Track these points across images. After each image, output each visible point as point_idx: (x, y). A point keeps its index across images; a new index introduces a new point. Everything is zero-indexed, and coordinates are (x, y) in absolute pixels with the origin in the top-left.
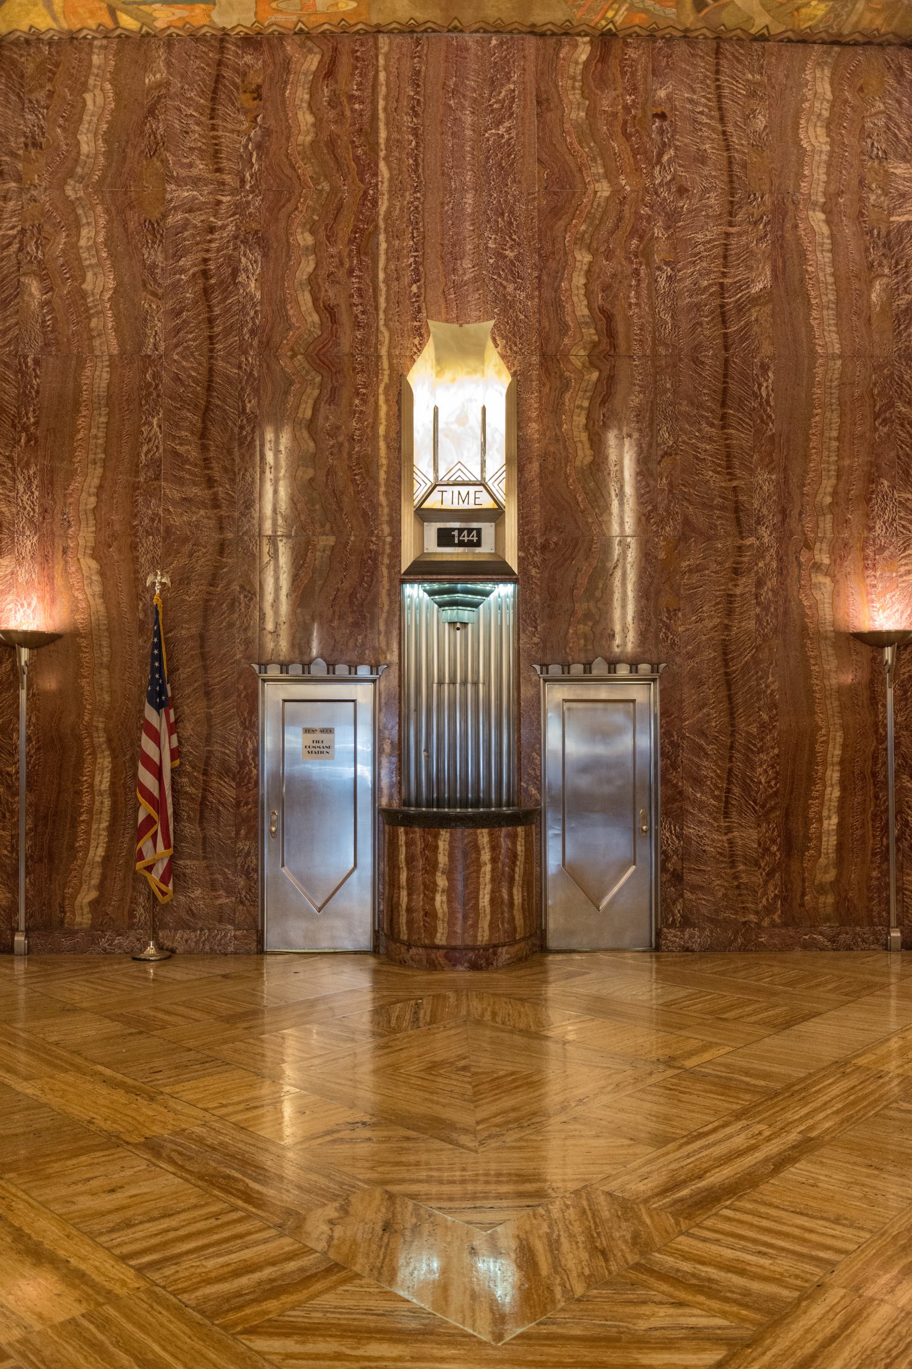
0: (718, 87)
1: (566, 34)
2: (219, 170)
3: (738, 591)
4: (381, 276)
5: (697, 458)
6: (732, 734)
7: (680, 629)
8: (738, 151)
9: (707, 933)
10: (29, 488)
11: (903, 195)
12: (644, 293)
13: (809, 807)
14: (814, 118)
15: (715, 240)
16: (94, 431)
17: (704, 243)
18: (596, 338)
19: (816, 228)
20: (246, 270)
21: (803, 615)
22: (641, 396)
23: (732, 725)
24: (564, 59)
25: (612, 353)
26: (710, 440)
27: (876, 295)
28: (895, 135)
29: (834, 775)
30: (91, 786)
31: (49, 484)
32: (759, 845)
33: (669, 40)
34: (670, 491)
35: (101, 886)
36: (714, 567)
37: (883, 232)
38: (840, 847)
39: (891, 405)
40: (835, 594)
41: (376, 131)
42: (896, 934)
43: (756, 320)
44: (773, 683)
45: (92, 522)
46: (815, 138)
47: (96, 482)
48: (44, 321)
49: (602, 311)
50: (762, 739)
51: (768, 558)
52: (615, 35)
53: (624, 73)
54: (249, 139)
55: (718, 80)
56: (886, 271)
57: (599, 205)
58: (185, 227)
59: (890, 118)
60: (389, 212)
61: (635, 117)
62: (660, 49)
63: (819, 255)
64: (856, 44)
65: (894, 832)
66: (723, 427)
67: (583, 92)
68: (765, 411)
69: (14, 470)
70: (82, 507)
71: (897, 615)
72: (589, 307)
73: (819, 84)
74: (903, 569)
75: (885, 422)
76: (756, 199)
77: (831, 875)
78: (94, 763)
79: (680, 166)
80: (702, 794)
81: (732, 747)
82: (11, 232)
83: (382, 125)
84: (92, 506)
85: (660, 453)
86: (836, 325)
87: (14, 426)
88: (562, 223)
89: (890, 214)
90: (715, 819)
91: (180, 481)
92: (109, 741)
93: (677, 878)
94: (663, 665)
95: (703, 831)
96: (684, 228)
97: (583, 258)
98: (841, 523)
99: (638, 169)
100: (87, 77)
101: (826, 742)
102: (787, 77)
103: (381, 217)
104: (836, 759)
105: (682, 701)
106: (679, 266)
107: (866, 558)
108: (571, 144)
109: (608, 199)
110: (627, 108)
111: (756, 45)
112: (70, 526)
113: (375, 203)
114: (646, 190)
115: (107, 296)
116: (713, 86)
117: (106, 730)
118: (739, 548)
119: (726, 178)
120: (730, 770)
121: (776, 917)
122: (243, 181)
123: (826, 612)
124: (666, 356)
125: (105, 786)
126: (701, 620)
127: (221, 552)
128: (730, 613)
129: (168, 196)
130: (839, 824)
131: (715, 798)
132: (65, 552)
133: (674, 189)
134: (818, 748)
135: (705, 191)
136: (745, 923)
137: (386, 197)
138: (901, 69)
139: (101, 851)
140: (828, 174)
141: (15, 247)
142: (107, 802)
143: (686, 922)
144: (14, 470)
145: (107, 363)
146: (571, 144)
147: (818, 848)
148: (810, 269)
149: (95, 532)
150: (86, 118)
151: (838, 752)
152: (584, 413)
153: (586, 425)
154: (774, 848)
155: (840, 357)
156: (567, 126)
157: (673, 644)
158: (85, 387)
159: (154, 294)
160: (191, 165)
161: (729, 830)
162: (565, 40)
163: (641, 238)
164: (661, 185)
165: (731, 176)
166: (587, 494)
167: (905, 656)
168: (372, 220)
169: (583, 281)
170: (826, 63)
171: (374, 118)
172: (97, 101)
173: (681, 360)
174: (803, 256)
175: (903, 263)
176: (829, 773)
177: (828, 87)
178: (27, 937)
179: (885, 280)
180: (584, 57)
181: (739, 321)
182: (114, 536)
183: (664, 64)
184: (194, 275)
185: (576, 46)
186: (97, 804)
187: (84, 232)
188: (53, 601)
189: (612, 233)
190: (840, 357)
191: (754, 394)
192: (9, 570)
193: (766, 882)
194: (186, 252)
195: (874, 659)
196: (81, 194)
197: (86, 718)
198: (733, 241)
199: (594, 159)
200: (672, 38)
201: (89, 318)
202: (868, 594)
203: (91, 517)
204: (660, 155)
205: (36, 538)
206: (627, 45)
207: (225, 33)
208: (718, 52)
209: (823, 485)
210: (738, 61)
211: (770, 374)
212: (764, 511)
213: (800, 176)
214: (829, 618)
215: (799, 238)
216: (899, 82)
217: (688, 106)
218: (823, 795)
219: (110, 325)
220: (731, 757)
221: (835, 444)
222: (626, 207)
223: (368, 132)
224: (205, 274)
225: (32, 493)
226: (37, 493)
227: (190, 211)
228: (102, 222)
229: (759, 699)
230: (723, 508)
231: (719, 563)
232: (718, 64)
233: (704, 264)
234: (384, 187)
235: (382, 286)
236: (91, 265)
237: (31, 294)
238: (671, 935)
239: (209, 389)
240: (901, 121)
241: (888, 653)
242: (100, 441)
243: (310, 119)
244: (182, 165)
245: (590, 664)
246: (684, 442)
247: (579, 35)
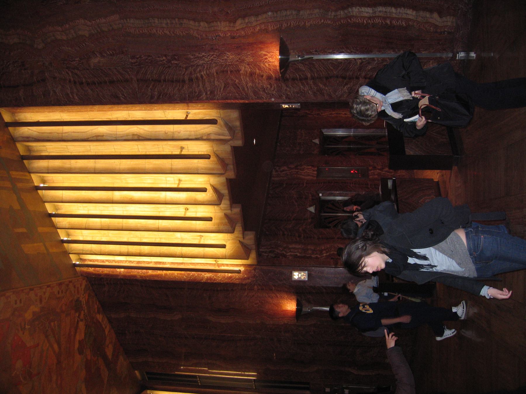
10: (201, 58)
16: (164, 25)
30: (370, 18)
35: (431, 11)
45: (215, 24)
47: (191, 22)
69: (192, 66)
78: (356, 17)
82: (70, 74)
84: (206, 25)
87: (169, 67)
92: (343, 8)
112: (219, 36)
117: (336, 11)
125: (370, 10)
132: (233, 38)
139: (410, 12)
141: (76, 71)
142: (380, 9)
144: (192, 66)
145: (125, 20)
149: (220, 22)
158: (141, 31)
186: (381, 14)
187: (59, 37)
188: (262, 43)
192: (247, 66)
197: (329, 22)
203: (212, 24)
219: (104, 20)
225: (203, 56)
226: (203, 54)
237: (99, 62)
242: (169, 22)
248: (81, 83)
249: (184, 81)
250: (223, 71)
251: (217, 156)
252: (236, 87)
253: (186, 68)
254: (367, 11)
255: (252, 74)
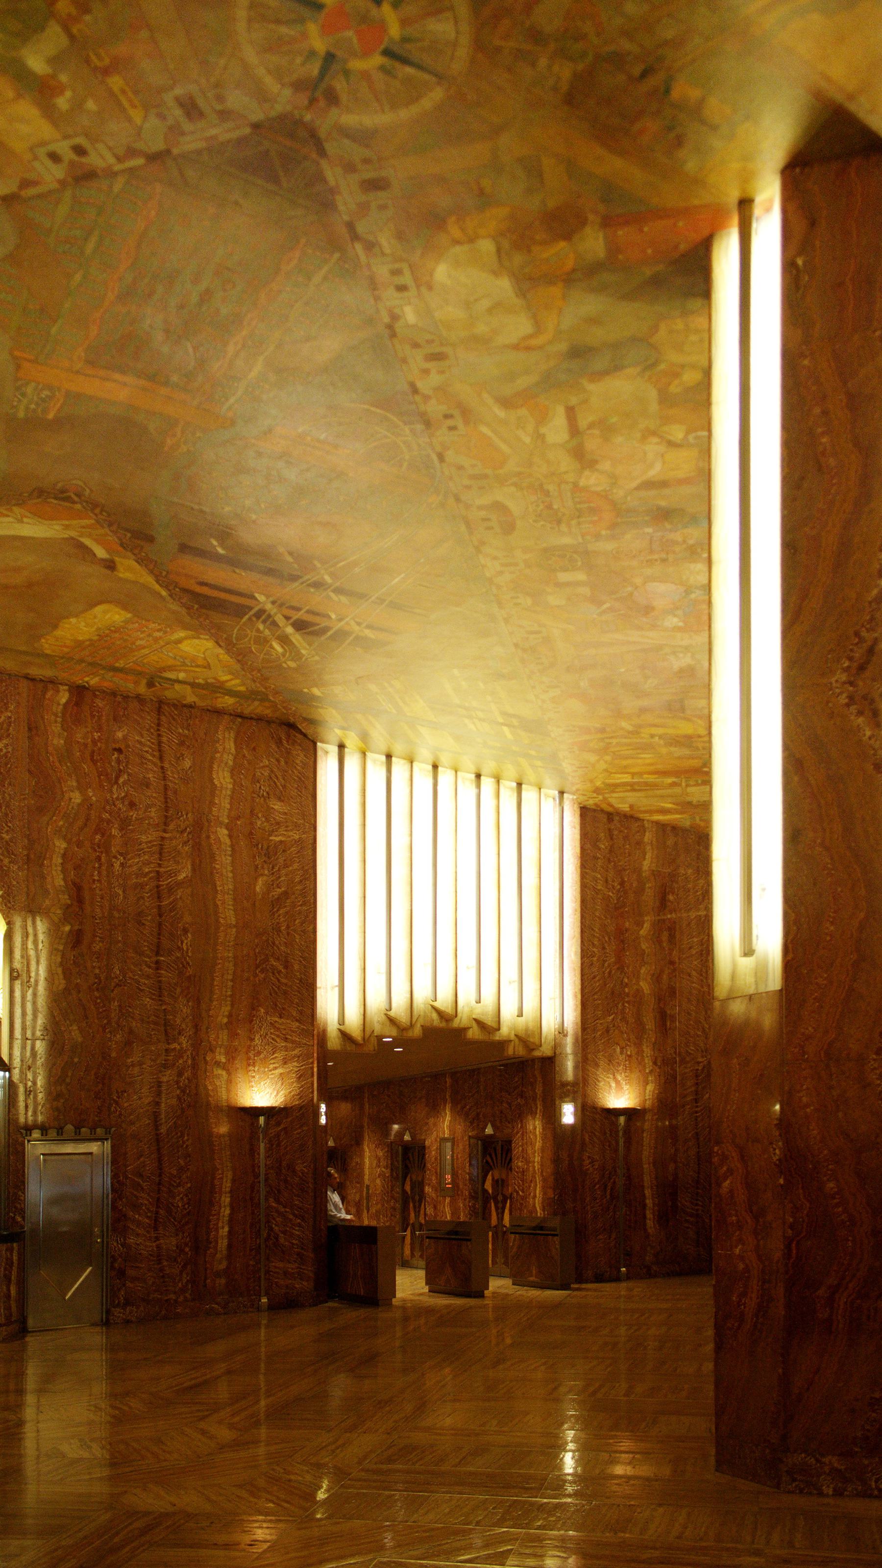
0: (159, 735)
1: (52, 682)
3: (165, 1079)
5: (138, 988)
6: (160, 1175)
7: (126, 1105)
8: (171, 781)
9: (142, 1308)
11: (278, 823)
12: (104, 873)
13: (210, 1221)
14: (223, 765)
15: (154, 841)
17: (146, 843)
18: (69, 902)
19: (222, 839)
21: (208, 1095)
22: (101, 944)
23: (161, 1169)
24: (49, 699)
25: (80, 913)
26: (148, 977)
27: (259, 887)
28: (275, 783)
29: (226, 1200)
32: (177, 1247)
33: (126, 698)
34: (120, 1011)
36: (149, 1063)
37: (265, 846)
38: (230, 1246)
39: (266, 960)
40: (229, 1081)
42: (264, 1300)
43: (181, 898)
44: (188, 1140)
46: (223, 778)
49: (74, 884)
50: (180, 1178)
51: (185, 1057)
52: (87, 689)
53: (93, 716)
55: (158, 730)
56: (266, 872)
57: (73, 808)
59: (272, 771)
61: (100, 749)
62: (119, 703)
63: (224, 858)
64: (251, 718)
65: (265, 1234)
66: (157, 969)
67: (62, 725)
68: (185, 959)
71: (268, 1096)
72: (64, 879)
73: (227, 744)
74: (271, 1066)
75: (262, 971)
76: (182, 816)
77: (223, 1265)
79: (131, 787)
80: (139, 1215)
81: (159, 1184)
85: (113, 984)
86: (233, 905)
88: (45, 819)
89: (270, 835)
90: (148, 1232)
93: (122, 1273)
94: (113, 1129)
95: (140, 1241)
96: (133, 831)
97: (61, 845)
98: (233, 1035)
99: (101, 786)
101: (222, 1178)
102: (205, 734)
104: (228, 1190)
105: (126, 1154)
106: (129, 857)
107: (249, 1058)
108: (53, 762)
109: (79, 805)
110: (94, 742)
111: (185, 710)
114: (107, 801)
116: (155, 733)
118: (166, 1050)
119: (163, 799)
120: (158, 1199)
121: (187, 1295)
123: (224, 1095)
124: (119, 918)
126: (140, 1098)
128: (159, 1094)
130: (230, 1232)
131: (148, 1217)
133: (126, 803)
134: (216, 1182)
135: (148, 806)
136: (167, 1300)
138: (280, 739)
140: (231, 804)
143: (127, 1303)
146: (53, 762)
147: (216, 1248)
148: (217, 866)
151: (229, 1185)
152: (60, 953)
153: (61, 963)
154: (187, 1249)
155: (235, 926)
156: (50, 749)
157: (121, 1114)
161: (157, 1239)
162: (50, 686)
163: (103, 835)
164: (117, 799)
165: (166, 798)
166: (60, 1010)
167: (272, 1122)
169: (60, 861)
170: (232, 728)
173: (129, 921)
174: (212, 857)
175: (276, 868)
176: (223, 1199)
177: (232, 745)
179: (265, 878)
180: (64, 701)
181: (169, 897)
183: (121, 713)
185: (58, 691)
189: (81, 829)
190: (235, 926)
191: (179, 948)
193: (181, 1273)
195: (252, 1124)
198: (167, 842)
199: (70, 775)
200: (128, 697)
202: (250, 1082)
204: (117, 778)
206: (95, 696)
208: (159, 711)
209: (223, 1010)
210: (174, 719)
211: (189, 935)
212: (184, 1026)
213: (212, 803)
214: (224, 1097)
215: (210, 845)
216: (278, 747)
217: (138, 746)
218: (219, 1214)
220: (159, 1190)
221: (230, 984)
222: (92, 812)
229: (178, 1151)
230: (155, 1023)
231: (153, 1060)
232: (159, 719)
233: (146, 857)
238: (117, 1312)
240: (279, 774)
241: (262, 1120)
245: (62, 1128)
246: (130, 978)
247: (61, 684)
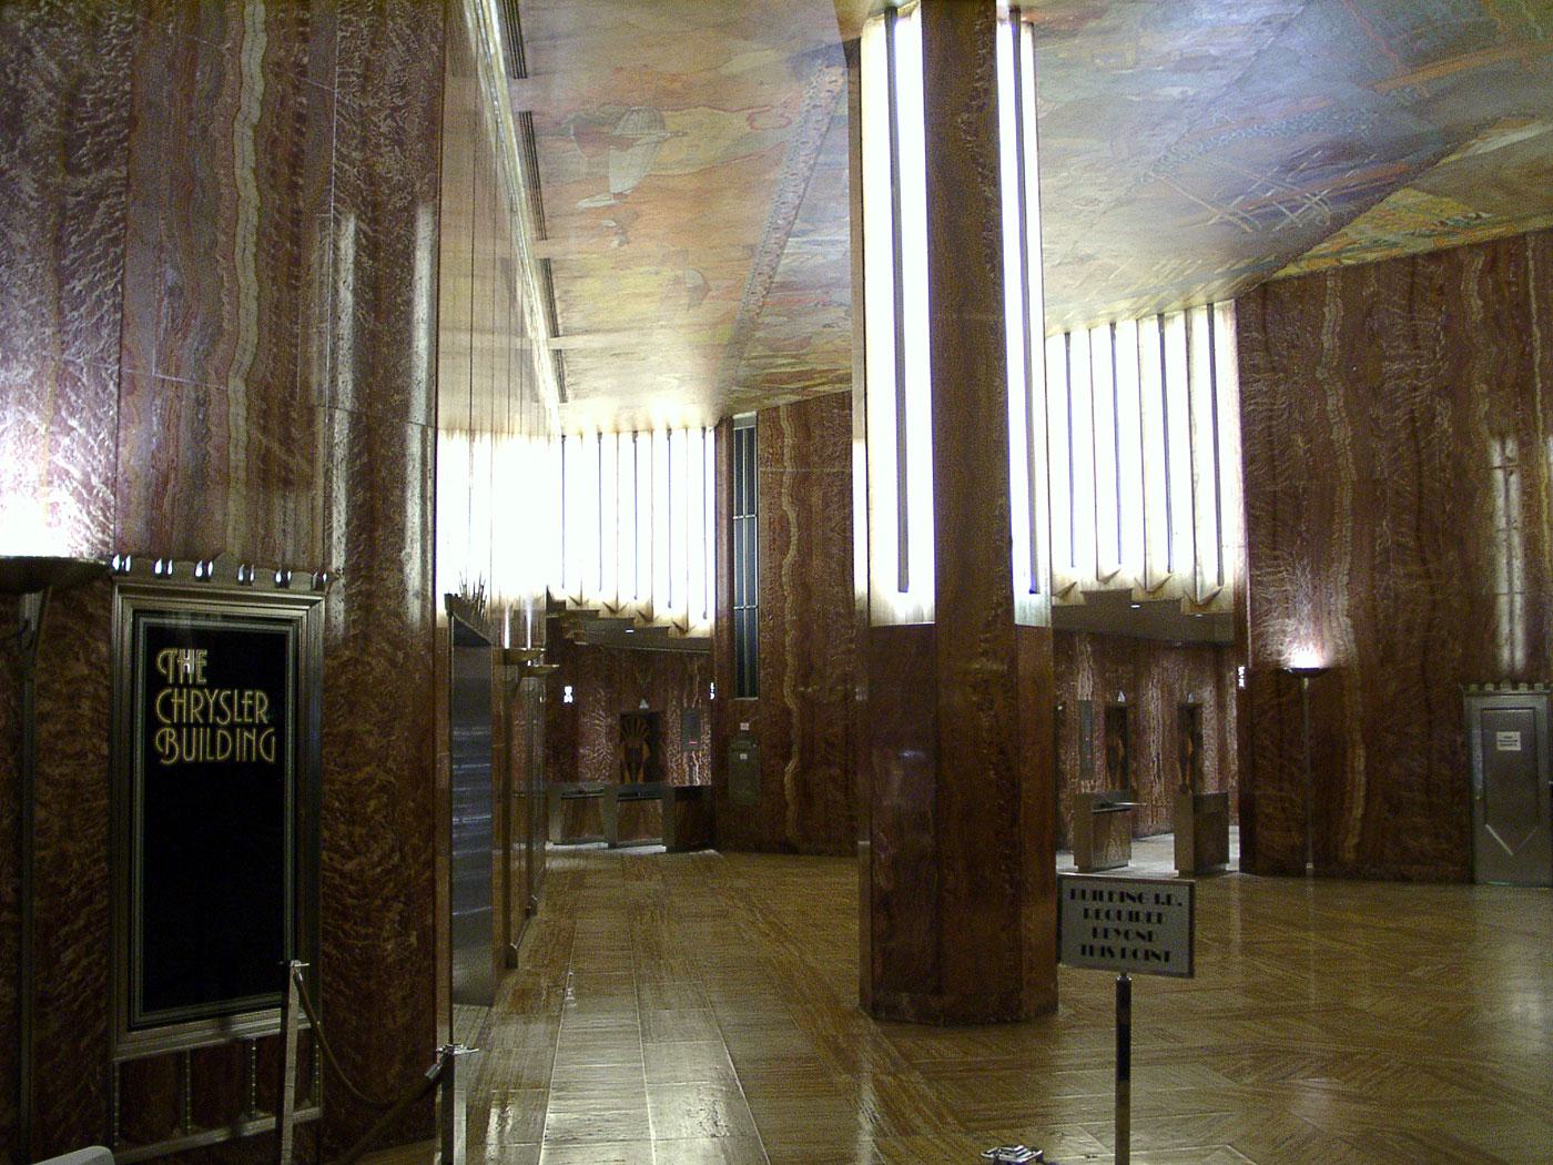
2: (1418, 348)
4: (1539, 407)
20: (1441, 414)
31: (1316, 572)
41: (1528, 304)
48: (1308, 462)
54: (1437, 324)
58: (1396, 391)
60: (1541, 364)
70: (1339, 584)
83: (1533, 300)
91: (1404, 563)
100: (1324, 296)
103: (1536, 365)
113: (1531, 355)
115: (1347, 442)
122: (1435, 353)
127: (1433, 608)
129: (1384, 370)
137: (1539, 351)
150: (1326, 324)
159: (1379, 437)
160: (1398, 347)
168: (1531, 368)
171: (1527, 294)
172: (1332, 312)
178: (1315, 866)
182: (1361, 601)
184: (1406, 420)
187: (1330, 401)
188: (1323, 647)
194: (1398, 407)
196: (1326, 375)
201: (1336, 458)
203: (1346, 589)
205: (1310, 606)
207: (1414, 257)
223: (1522, 305)
224: (1413, 420)
227: (1399, 378)
228: (1341, 393)
234: (1537, 344)
235: (1540, 415)
236: (1336, 423)
239: (1420, 498)
243: (1480, 303)
244: (1393, 348)
248: (1270, 418)
249: (1275, 549)
250: (1287, 598)
251: (1169, 578)
252: (1268, 612)
253: (1291, 554)
254: (1360, 764)
255: (1284, 632)
